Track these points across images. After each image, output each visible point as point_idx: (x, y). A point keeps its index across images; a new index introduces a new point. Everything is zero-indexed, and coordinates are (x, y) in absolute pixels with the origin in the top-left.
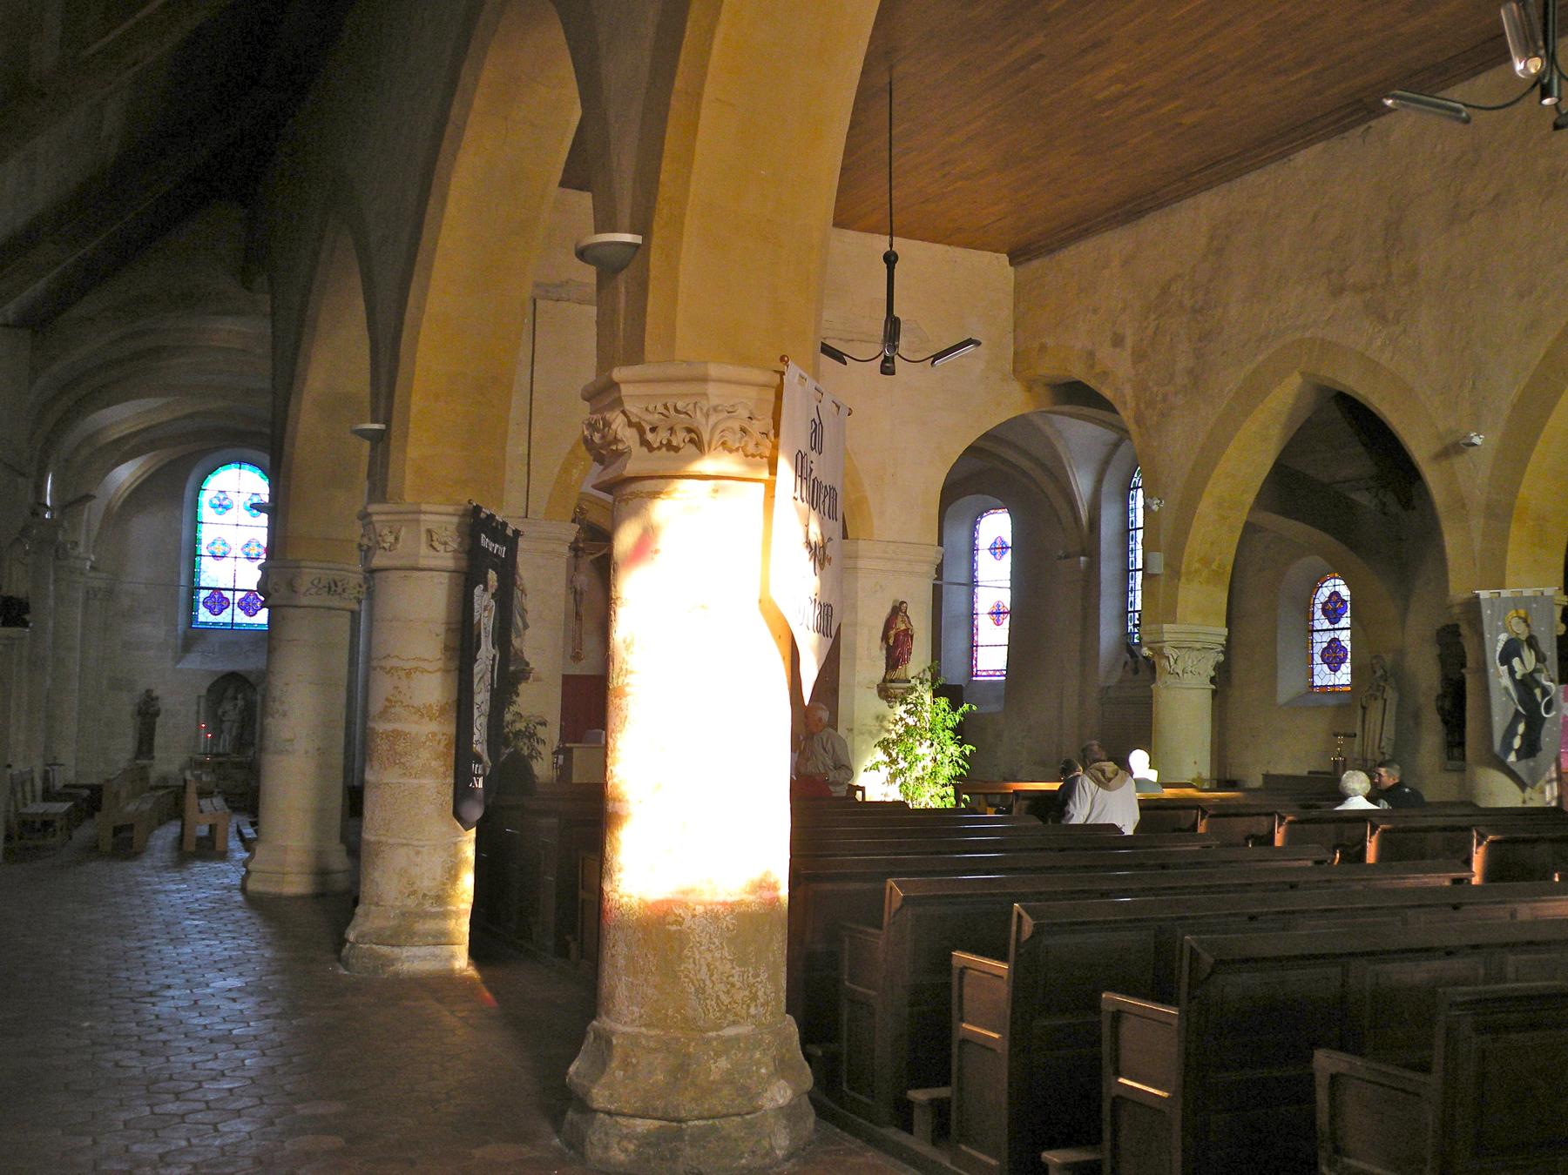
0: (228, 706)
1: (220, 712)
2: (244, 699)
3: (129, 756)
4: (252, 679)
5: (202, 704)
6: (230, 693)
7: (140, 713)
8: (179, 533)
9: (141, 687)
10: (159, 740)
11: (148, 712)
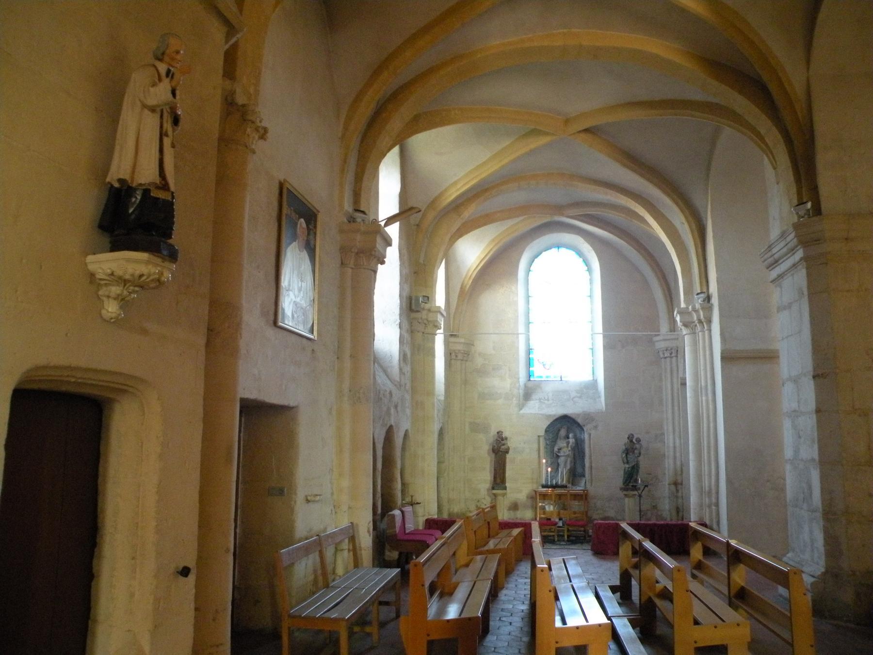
0: (561, 443)
1: (556, 449)
2: (575, 437)
3: (488, 485)
4: (579, 421)
5: (542, 439)
6: (563, 433)
7: (494, 451)
8: (516, 303)
9: (493, 432)
10: (509, 473)
11: (500, 451)
